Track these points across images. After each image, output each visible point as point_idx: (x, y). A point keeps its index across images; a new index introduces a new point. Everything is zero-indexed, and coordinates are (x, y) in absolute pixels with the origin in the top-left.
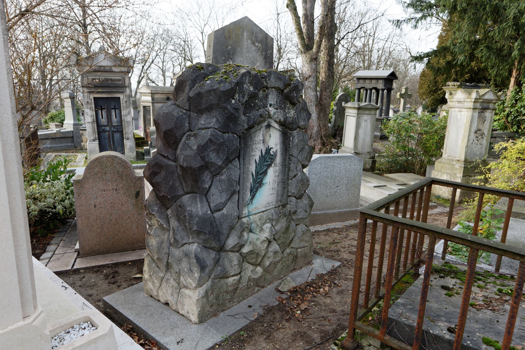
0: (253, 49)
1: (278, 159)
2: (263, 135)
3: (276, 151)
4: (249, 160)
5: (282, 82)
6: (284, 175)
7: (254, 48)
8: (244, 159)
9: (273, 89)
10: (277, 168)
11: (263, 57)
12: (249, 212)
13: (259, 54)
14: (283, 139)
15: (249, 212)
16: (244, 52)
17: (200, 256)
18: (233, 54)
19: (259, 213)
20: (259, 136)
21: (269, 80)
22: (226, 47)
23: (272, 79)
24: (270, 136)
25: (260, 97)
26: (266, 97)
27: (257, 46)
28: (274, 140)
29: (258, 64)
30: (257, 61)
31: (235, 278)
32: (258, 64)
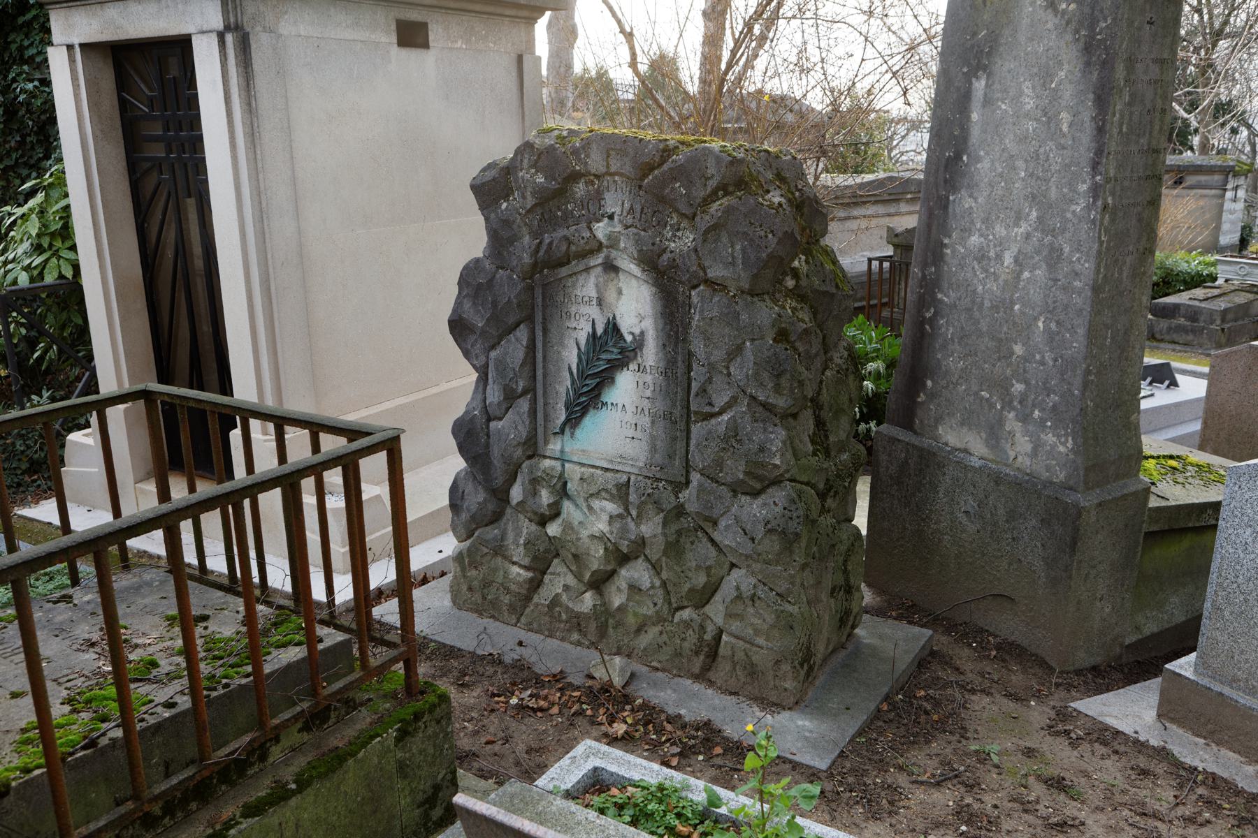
0: (1050, 25)
1: (651, 354)
2: (597, 286)
3: (642, 333)
4: (562, 336)
5: (626, 159)
6: (674, 405)
7: (1051, 21)
8: (545, 331)
9: (617, 178)
10: (649, 378)
11: (1081, 45)
12: (562, 451)
13: (1069, 37)
14: (665, 307)
15: (562, 451)
16: (1022, 39)
17: (461, 485)
18: (989, 54)
19: (596, 467)
20: (587, 287)
21: (587, 156)
22: (975, 34)
23: (593, 156)
24: (620, 292)
25: (578, 195)
26: (598, 197)
27: (1064, 12)
28: (634, 306)
29: (1062, 74)
30: (1060, 63)
31: (522, 571)
32: (1062, 74)
